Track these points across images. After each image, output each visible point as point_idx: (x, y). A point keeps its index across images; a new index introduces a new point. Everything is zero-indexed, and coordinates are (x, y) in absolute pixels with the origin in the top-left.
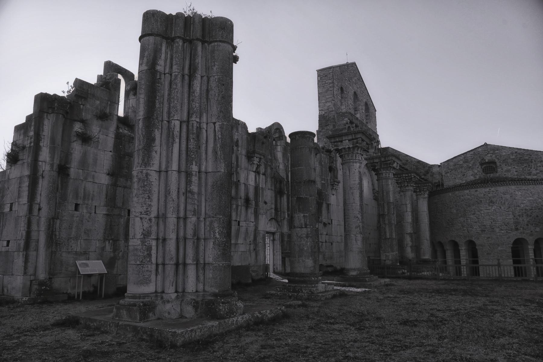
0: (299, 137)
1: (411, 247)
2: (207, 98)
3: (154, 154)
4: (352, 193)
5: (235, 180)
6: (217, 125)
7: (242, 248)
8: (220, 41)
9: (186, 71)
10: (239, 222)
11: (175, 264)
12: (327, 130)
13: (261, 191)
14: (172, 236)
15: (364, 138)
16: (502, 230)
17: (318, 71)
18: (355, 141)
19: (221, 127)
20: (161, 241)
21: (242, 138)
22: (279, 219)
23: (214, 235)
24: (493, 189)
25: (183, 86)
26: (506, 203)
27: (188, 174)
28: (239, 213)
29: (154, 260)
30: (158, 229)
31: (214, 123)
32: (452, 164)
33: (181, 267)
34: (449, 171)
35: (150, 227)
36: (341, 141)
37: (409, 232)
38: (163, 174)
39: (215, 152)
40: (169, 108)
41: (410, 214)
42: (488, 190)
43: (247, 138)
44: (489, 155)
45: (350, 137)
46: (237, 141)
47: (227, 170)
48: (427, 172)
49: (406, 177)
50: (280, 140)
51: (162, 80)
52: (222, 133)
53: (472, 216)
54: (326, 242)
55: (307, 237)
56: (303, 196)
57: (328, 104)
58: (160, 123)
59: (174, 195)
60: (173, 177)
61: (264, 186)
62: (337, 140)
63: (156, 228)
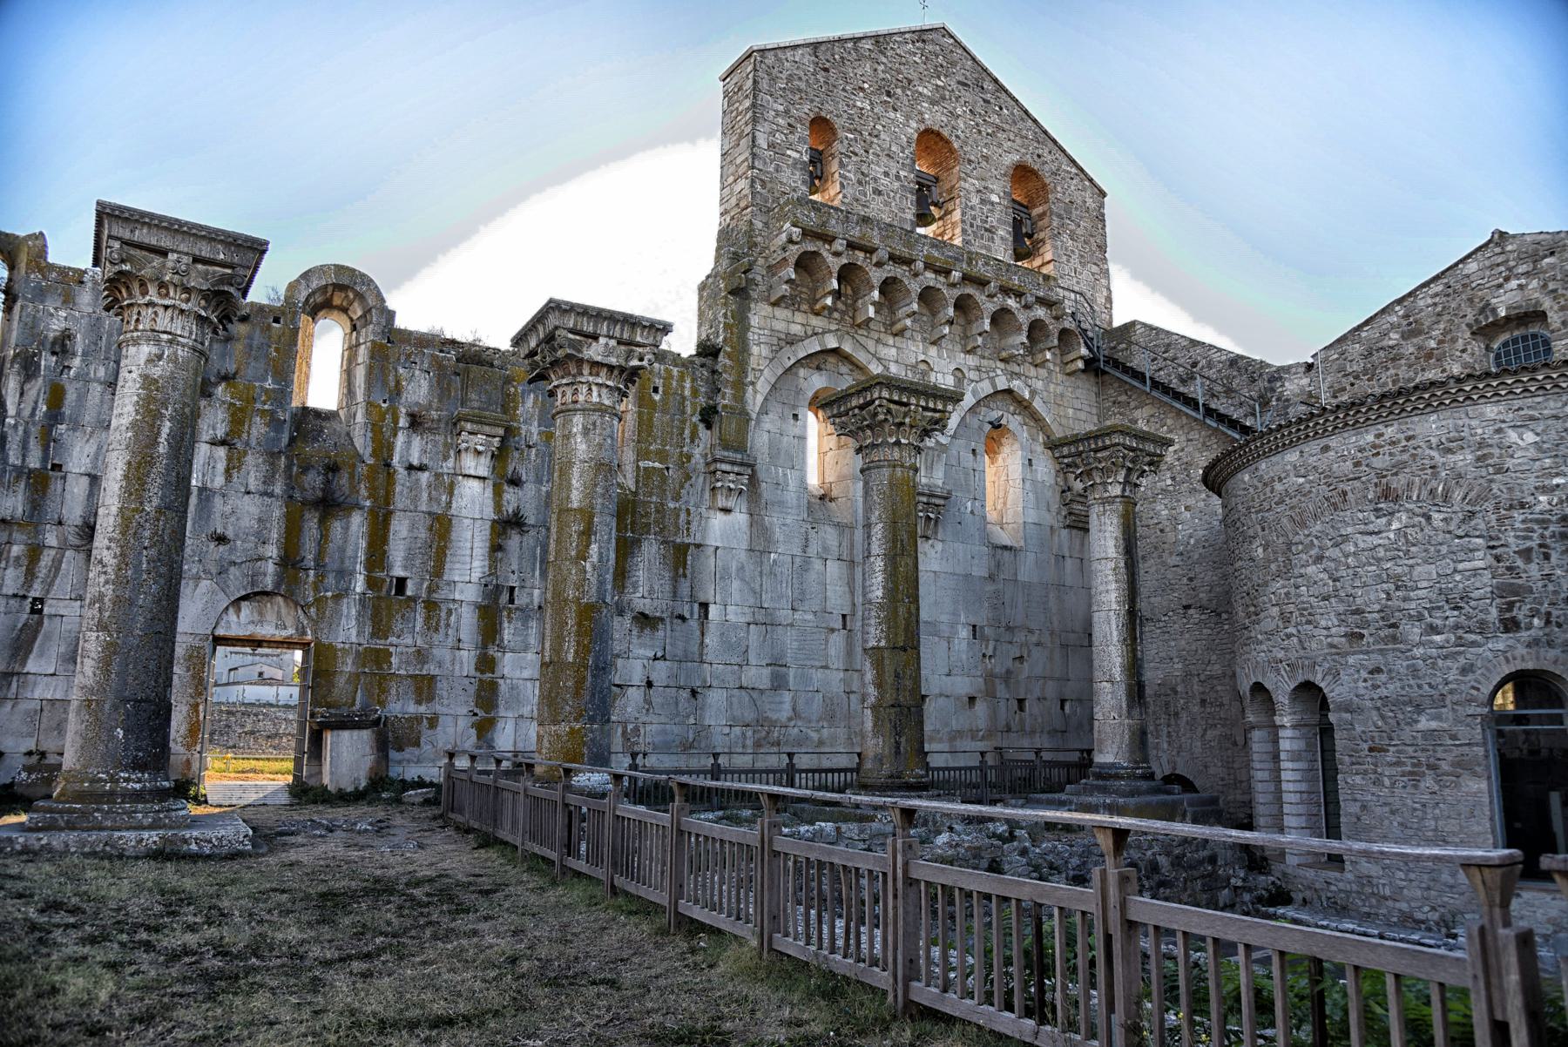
5: (34, 462)
13: (193, 500)
16: (1433, 629)
24: (1390, 432)
26: (1457, 495)
32: (1356, 349)
34: (1345, 382)
41: (879, 564)
42: (1370, 438)
44: (1514, 283)
53: (1311, 570)
54: (650, 684)
61: (219, 481)
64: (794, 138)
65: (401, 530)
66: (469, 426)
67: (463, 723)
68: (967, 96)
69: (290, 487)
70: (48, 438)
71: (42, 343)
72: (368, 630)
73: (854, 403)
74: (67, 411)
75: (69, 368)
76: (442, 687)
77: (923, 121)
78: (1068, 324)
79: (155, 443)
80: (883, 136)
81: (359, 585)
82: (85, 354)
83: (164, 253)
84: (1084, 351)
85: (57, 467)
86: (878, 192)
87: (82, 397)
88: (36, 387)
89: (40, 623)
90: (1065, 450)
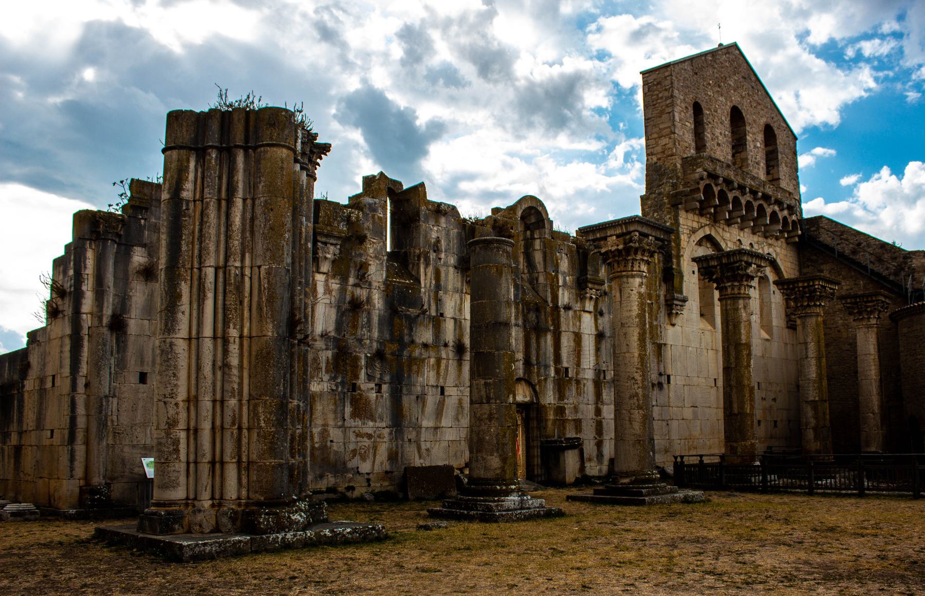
0: (481, 248)
1: (815, 429)
2: (252, 233)
3: (180, 315)
4: (625, 334)
5: (434, 314)
6: (263, 268)
7: (450, 435)
8: (268, 145)
9: (223, 195)
10: (442, 389)
11: (209, 462)
12: (660, 194)
14: (206, 426)
15: (645, 230)
17: (643, 73)
18: (628, 237)
19: (268, 273)
20: (192, 432)
21: (448, 234)
22: (535, 380)
23: (259, 424)
25: (219, 217)
27: (226, 341)
28: (442, 372)
29: (183, 456)
30: (189, 416)
31: (259, 267)
33: (218, 466)
35: (177, 413)
36: (605, 238)
37: (811, 398)
38: (194, 342)
39: (260, 308)
40: (200, 251)
41: (813, 362)
43: (459, 234)
45: (618, 231)
46: (438, 241)
47: (278, 333)
48: (900, 268)
49: (804, 287)
50: (538, 228)
51: (191, 211)
52: (269, 281)
55: (490, 418)
56: (486, 350)
57: (664, 141)
58: (189, 271)
59: (207, 369)
60: (208, 345)
62: (598, 236)
63: (185, 415)
64: (688, 115)
65: (566, 342)
66: (590, 285)
67: (593, 443)
68: (746, 85)
69: (525, 321)
70: (438, 301)
71: (430, 246)
72: (557, 396)
73: (800, 285)
74: (442, 283)
75: (440, 259)
76: (584, 424)
77: (731, 101)
78: (794, 217)
79: (645, 325)
80: (719, 111)
81: (552, 373)
82: (446, 251)
83: (647, 236)
84: (800, 232)
85: (442, 315)
86: (719, 145)
87: (447, 275)
88: (430, 269)
89: (444, 400)
90: (849, 301)
